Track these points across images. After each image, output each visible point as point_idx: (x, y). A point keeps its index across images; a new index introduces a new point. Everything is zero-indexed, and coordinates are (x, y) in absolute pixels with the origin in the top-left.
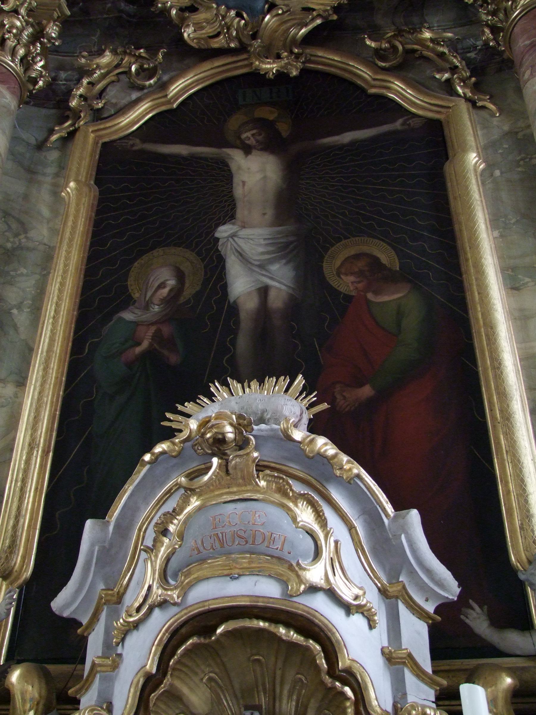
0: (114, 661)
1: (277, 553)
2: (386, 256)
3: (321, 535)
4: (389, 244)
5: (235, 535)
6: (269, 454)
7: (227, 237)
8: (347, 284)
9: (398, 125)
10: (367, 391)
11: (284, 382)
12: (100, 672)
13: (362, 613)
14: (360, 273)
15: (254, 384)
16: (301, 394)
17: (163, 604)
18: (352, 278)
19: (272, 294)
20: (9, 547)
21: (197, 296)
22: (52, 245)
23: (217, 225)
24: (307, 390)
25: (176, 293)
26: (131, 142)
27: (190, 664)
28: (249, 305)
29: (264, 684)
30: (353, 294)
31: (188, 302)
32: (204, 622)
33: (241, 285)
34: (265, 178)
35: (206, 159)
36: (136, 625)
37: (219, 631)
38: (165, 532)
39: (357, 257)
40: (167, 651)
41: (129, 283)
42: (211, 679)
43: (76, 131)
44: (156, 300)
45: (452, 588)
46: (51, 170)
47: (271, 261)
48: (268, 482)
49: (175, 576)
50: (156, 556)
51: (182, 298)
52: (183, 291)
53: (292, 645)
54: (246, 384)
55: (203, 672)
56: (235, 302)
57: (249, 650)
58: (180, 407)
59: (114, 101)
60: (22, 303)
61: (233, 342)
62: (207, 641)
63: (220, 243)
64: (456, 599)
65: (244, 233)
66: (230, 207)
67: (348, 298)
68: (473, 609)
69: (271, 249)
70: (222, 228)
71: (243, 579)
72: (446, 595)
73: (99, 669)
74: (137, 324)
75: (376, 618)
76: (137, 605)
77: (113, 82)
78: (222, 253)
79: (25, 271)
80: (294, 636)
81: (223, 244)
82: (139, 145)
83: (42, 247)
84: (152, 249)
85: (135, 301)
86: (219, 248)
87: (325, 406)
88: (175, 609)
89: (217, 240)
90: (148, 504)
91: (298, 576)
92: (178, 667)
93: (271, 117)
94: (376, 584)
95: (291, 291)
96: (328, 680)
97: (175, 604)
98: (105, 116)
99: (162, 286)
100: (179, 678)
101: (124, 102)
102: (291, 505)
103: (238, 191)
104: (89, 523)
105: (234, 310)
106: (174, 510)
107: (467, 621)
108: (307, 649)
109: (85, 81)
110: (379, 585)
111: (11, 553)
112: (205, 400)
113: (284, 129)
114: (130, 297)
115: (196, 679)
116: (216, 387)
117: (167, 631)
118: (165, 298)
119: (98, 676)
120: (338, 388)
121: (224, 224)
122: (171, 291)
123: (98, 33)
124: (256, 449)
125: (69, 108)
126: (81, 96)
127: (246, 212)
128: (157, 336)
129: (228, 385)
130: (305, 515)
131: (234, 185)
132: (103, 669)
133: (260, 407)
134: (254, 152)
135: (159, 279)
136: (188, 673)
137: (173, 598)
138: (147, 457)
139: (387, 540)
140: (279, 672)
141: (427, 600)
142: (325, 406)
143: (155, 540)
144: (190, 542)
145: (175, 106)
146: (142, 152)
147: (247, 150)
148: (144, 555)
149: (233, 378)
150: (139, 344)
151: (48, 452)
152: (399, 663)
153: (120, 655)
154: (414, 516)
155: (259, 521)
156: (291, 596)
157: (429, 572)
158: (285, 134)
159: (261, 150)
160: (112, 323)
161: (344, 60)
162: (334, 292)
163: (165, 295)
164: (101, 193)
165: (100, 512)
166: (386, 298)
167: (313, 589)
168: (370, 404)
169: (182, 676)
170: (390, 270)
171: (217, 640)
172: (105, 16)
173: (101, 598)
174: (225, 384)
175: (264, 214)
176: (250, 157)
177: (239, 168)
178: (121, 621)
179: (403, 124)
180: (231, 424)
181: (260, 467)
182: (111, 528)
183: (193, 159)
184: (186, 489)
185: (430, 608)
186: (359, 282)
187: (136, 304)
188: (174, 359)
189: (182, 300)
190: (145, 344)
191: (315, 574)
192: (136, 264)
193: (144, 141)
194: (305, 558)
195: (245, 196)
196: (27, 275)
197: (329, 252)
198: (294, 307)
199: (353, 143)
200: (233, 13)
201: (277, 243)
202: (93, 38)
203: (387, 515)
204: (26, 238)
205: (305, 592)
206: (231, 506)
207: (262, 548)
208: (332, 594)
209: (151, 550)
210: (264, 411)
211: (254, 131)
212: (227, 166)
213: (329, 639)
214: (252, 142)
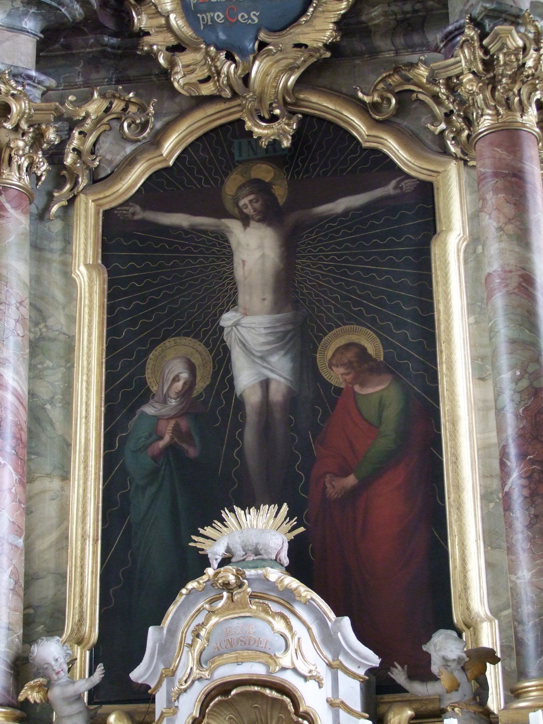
0: (174, 710)
1: (263, 650)
2: (373, 346)
3: (289, 635)
4: (376, 333)
5: (239, 640)
6: (258, 588)
7: (231, 326)
8: (337, 376)
9: (389, 189)
10: (351, 480)
11: (274, 508)
12: (166, 716)
13: (315, 679)
14: (349, 365)
15: (253, 510)
16: (285, 519)
17: (200, 679)
18: (342, 370)
19: (273, 387)
20: (79, 621)
21: (209, 388)
22: (71, 335)
23: (221, 313)
24: (290, 515)
25: (190, 385)
26: (131, 210)
27: (218, 711)
28: (253, 399)
29: (261, 720)
30: (343, 386)
31: (201, 395)
32: (224, 688)
33: (246, 378)
34: (263, 256)
35: (205, 232)
36: (185, 690)
37: (233, 693)
38: (198, 636)
39: (348, 346)
40: (204, 705)
41: (147, 376)
42: (230, 718)
43: (75, 197)
44: (172, 395)
45: (375, 660)
46: (57, 245)
47: (271, 352)
48: (257, 606)
49: (206, 663)
50: (194, 650)
51: (195, 392)
52: (195, 385)
53: (274, 700)
54: (247, 511)
55: (225, 714)
56: (241, 395)
57: (251, 702)
58: (201, 531)
59: (109, 157)
60: (53, 398)
61: (241, 435)
62: (226, 699)
63: (225, 333)
64: (378, 665)
65: (247, 321)
66: (232, 292)
67: (339, 391)
68: (396, 668)
69: (271, 338)
70: (226, 316)
71: (244, 664)
72: (371, 664)
73: (166, 715)
74: (157, 418)
75: (323, 682)
76: (185, 679)
77: (105, 131)
78: (227, 344)
79: (51, 364)
80: (275, 694)
81: (228, 333)
82: (140, 214)
83: (62, 337)
84: (164, 339)
85: (154, 395)
86: (225, 339)
87: (302, 529)
88: (207, 682)
89: (222, 329)
90: (186, 616)
91: (275, 662)
92: (211, 713)
93: (268, 179)
94: (325, 661)
95: (289, 385)
96: (294, 717)
97: (207, 679)
98: (102, 175)
99: (176, 379)
100: (212, 719)
101: (119, 158)
102: (270, 619)
103: (239, 273)
104: (151, 629)
105: (240, 403)
106: (203, 623)
107: (392, 676)
108: (283, 701)
109: (76, 133)
110: (327, 661)
111: (81, 625)
112: (219, 524)
113: (280, 192)
114: (149, 391)
115: (222, 719)
116: (226, 514)
117: (203, 694)
118: (180, 391)
119: (165, 719)
120: (328, 478)
121: (228, 311)
122: (185, 384)
123: (82, 64)
124: (249, 586)
125: (65, 167)
126: (74, 149)
127: (247, 298)
128: (176, 430)
129: (234, 512)
130: (279, 625)
131: (235, 265)
132: (168, 715)
133: (255, 541)
134: (253, 224)
135: (173, 368)
136: (217, 715)
137: (205, 676)
138: (184, 591)
139: (330, 635)
140: (269, 713)
141: (359, 667)
142: (302, 529)
143: (193, 641)
144: (213, 644)
145: (171, 163)
146: (143, 222)
147: (245, 220)
148: (186, 649)
149: (237, 506)
150: (161, 438)
151: (97, 540)
152: (337, 707)
153: (177, 707)
154: (346, 621)
155: (252, 631)
156: (272, 673)
157: (357, 652)
158: (281, 201)
159: (259, 221)
160: (137, 416)
161: (338, 109)
162: (327, 385)
163: (180, 388)
164: (110, 273)
165: (158, 622)
166: (369, 390)
167: (284, 669)
168: (354, 493)
169: (214, 717)
170: (375, 360)
171: (232, 698)
172: (88, 50)
173: (162, 674)
174: (232, 511)
175: (264, 299)
176: (248, 229)
177: (239, 243)
178: (176, 688)
179: (396, 188)
180: (233, 574)
181: (252, 596)
182: (165, 631)
183: (194, 232)
184: (209, 612)
185: (361, 672)
186: (348, 374)
187: (156, 398)
188: (192, 452)
189: (195, 394)
190: (167, 438)
191: (285, 660)
192: (151, 356)
193: (145, 208)
194: (279, 650)
195: (245, 279)
196: (53, 368)
197: (322, 342)
198: (292, 400)
199: (346, 213)
200: (222, 56)
201: (277, 333)
202: (77, 68)
203: (330, 620)
204: (46, 326)
205: (279, 670)
206: (236, 621)
207: (254, 647)
208: (295, 670)
209: (191, 646)
210: (257, 544)
211: (251, 197)
212: (227, 241)
213: (295, 695)
214: (249, 211)
